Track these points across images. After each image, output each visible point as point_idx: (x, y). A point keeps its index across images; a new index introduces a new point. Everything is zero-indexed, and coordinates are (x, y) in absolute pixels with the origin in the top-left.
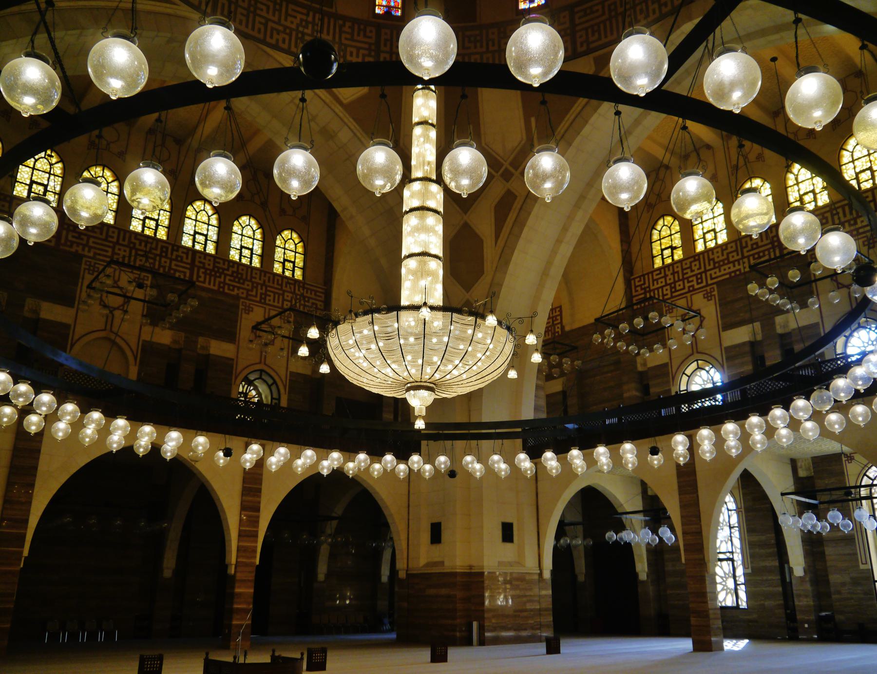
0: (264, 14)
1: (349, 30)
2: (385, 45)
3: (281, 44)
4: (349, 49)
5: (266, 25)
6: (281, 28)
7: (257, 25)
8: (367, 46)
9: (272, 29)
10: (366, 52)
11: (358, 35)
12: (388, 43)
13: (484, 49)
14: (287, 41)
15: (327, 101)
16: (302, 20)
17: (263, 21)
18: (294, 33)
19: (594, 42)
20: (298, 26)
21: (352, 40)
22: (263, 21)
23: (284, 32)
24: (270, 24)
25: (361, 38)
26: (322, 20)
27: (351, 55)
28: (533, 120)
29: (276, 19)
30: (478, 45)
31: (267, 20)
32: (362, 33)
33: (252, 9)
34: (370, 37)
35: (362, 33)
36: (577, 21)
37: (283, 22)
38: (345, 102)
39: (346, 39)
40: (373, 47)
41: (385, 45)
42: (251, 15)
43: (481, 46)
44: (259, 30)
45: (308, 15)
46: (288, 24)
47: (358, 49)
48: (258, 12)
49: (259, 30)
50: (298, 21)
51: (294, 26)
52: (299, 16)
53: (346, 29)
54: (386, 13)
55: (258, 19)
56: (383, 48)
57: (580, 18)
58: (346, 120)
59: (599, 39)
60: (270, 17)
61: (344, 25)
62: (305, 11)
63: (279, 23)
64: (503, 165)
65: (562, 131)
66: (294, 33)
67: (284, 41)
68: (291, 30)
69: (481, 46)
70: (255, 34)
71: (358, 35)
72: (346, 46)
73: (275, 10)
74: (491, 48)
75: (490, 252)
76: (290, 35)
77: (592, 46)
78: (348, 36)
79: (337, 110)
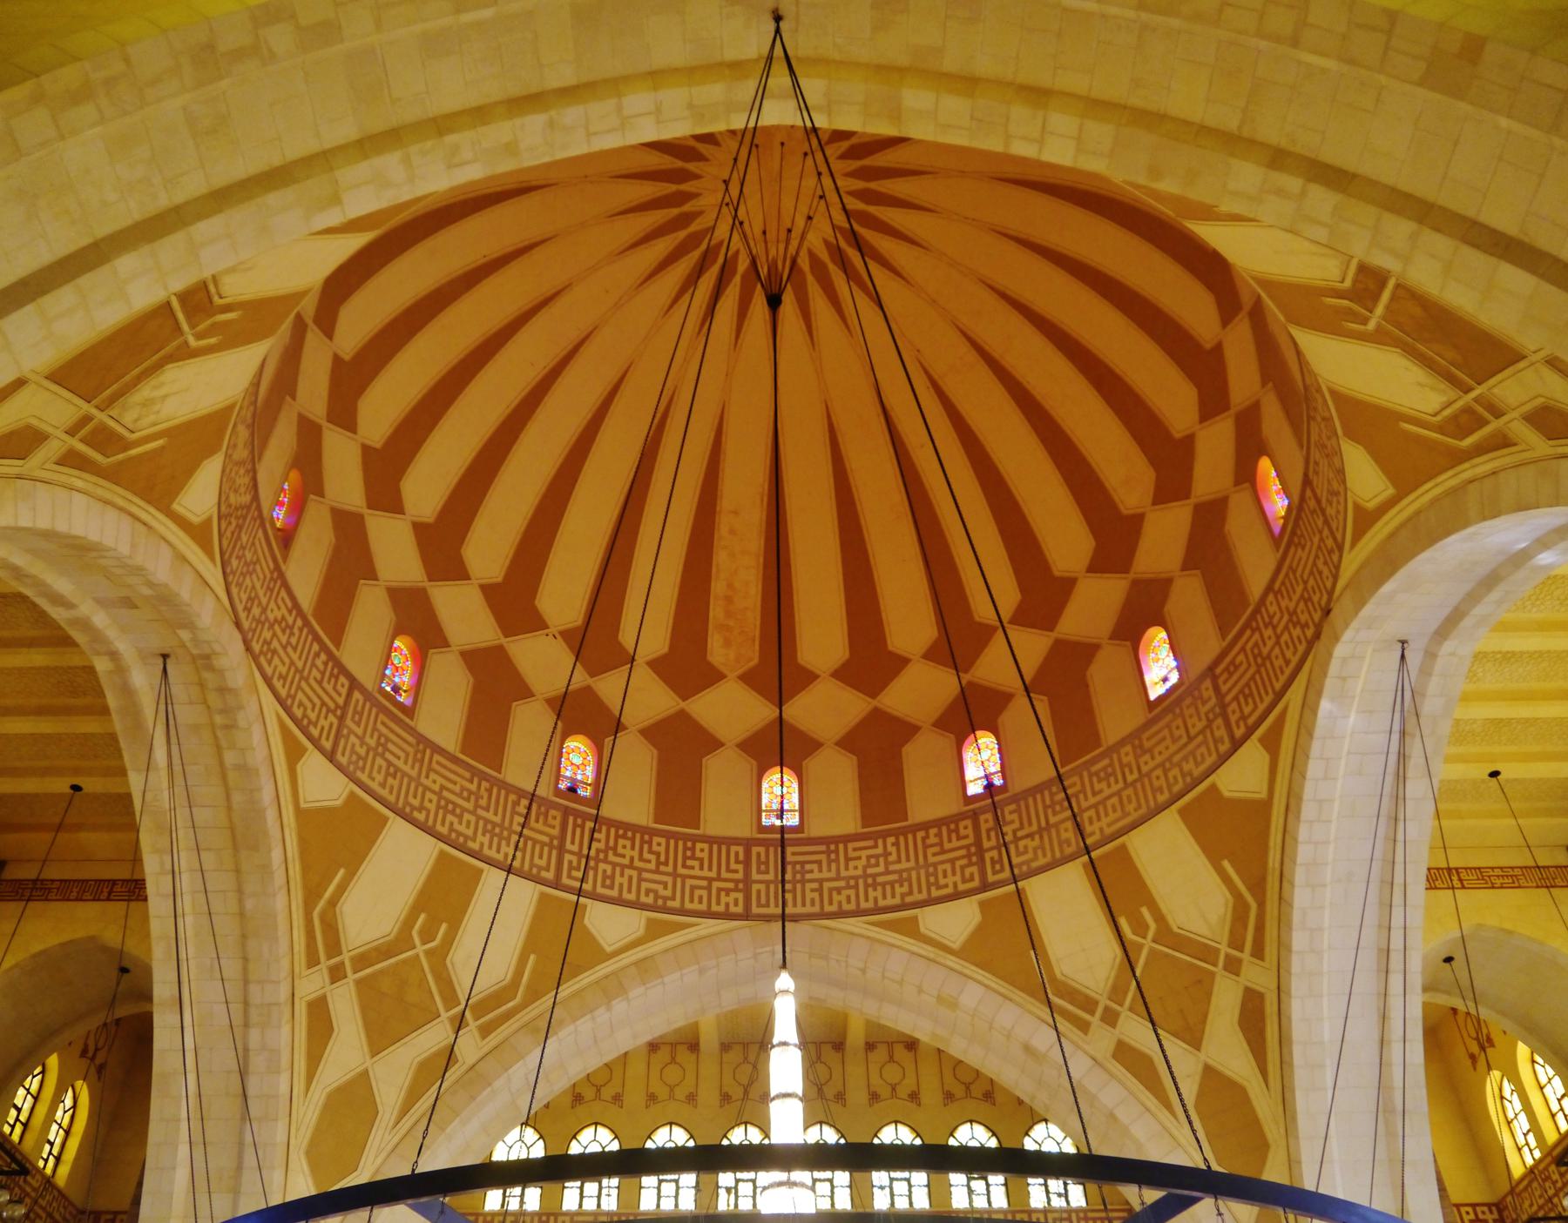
0: (816, 875)
1: (936, 840)
2: (989, 838)
3: (846, 907)
4: (940, 868)
5: (820, 890)
6: (842, 884)
7: (809, 895)
8: (963, 852)
9: (831, 890)
10: (964, 862)
11: (950, 841)
12: (993, 834)
13: (1121, 784)
14: (853, 898)
15: (932, 956)
16: (868, 857)
17: (815, 885)
18: (861, 882)
19: (1251, 714)
20: (865, 868)
21: (943, 852)
22: (815, 885)
23: (848, 887)
24: (826, 885)
25: (955, 844)
26: (896, 844)
27: (945, 876)
28: (1226, 864)
29: (833, 874)
30: (1112, 780)
31: (821, 881)
32: (954, 836)
33: (798, 877)
34: (966, 837)
35: (954, 836)
36: (1224, 688)
37: (843, 873)
38: (956, 946)
39: (934, 855)
40: (973, 849)
41: (989, 838)
42: (799, 886)
43: (1117, 782)
44: (813, 904)
45: (876, 846)
46: (852, 872)
47: (952, 861)
48: (808, 876)
49: (813, 901)
50: (863, 861)
51: (859, 872)
52: (864, 854)
53: (933, 840)
54: (986, 787)
55: (809, 886)
56: (986, 844)
57: (1225, 682)
58: (966, 971)
59: (1256, 707)
60: (825, 875)
61: (927, 837)
62: (870, 843)
63: (838, 878)
64: (1217, 951)
65: (1277, 865)
66: (861, 882)
67: (849, 901)
68: (856, 878)
69: (1117, 782)
70: (808, 909)
71: (950, 841)
72: (935, 865)
73: (830, 862)
74: (1130, 778)
75: (1264, 1105)
76: (856, 887)
77: (1251, 721)
78: (936, 849)
79: (950, 963)
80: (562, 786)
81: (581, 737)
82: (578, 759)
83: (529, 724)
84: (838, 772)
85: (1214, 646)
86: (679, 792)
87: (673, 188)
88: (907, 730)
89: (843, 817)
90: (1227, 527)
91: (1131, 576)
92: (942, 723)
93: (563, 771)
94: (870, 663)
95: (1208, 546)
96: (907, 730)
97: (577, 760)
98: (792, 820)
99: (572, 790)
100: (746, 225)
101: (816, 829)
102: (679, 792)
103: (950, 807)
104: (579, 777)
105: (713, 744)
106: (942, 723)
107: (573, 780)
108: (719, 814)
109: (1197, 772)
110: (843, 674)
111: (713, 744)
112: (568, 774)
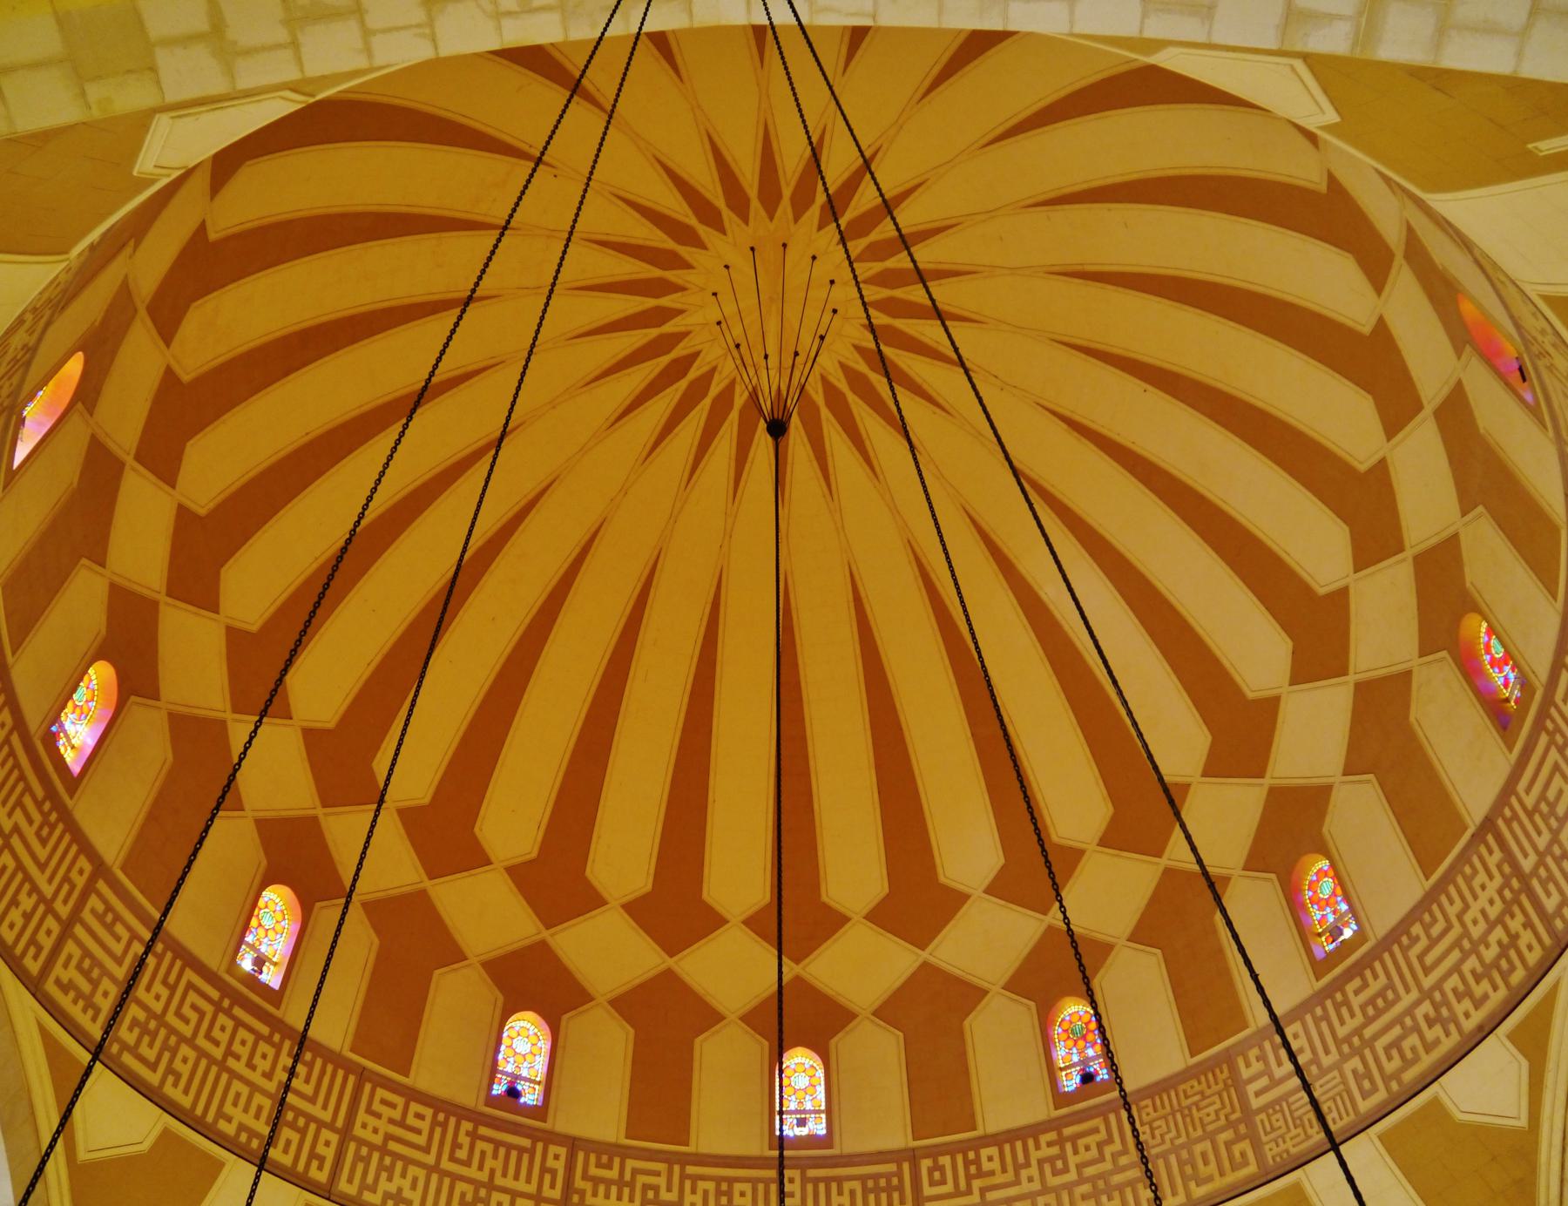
80: (498, 1089)
81: (530, 1015)
82: (525, 1046)
83: (455, 994)
84: (878, 1051)
85: (1410, 886)
86: (661, 1093)
87: (651, 303)
88: (968, 995)
89: (889, 1128)
90: (1413, 716)
91: (1267, 781)
92: (1018, 984)
93: (501, 1062)
94: (918, 902)
95: (1383, 734)
96: (968, 995)
97: (522, 1046)
98: (818, 1127)
99: (513, 1093)
100: (743, 348)
101: (848, 1144)
102: (661, 1093)
103: (1039, 1109)
104: (524, 1073)
105: (710, 1017)
106: (1018, 984)
107: (516, 1077)
108: (719, 1125)
109: (1410, 1075)
110: (880, 916)
111: (710, 1017)
112: (509, 1068)
